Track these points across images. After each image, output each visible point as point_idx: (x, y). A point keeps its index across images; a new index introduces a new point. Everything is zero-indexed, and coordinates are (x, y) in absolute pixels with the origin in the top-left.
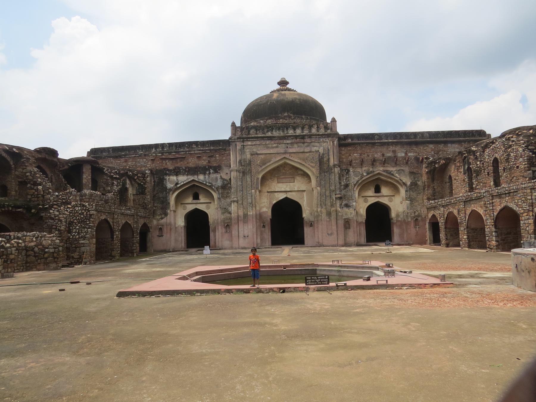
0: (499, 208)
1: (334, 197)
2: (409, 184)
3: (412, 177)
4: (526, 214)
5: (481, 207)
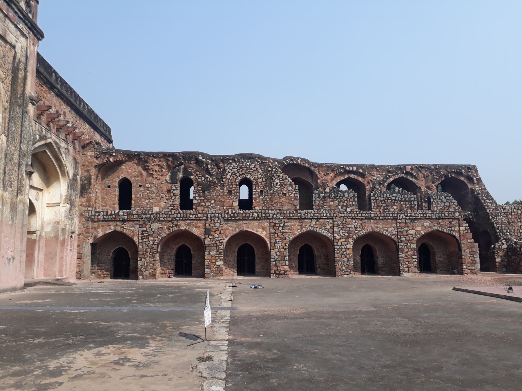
0: (297, 233)
1: (24, 168)
2: (71, 175)
3: (74, 166)
4: (344, 240)
5: (263, 229)
